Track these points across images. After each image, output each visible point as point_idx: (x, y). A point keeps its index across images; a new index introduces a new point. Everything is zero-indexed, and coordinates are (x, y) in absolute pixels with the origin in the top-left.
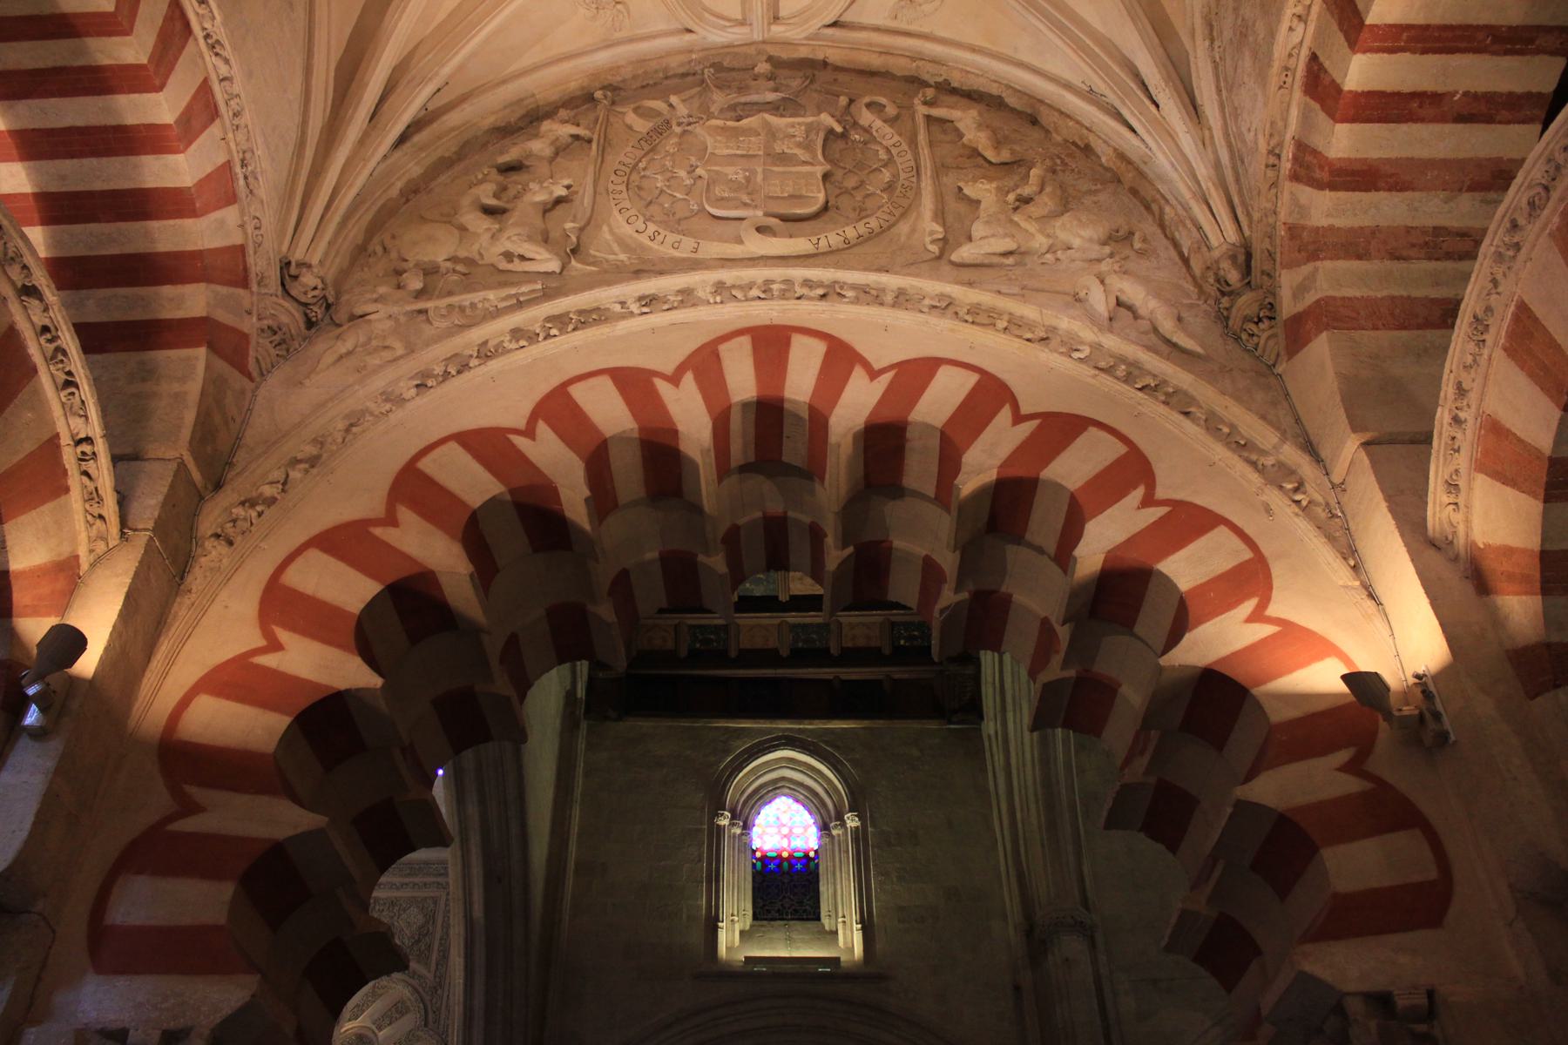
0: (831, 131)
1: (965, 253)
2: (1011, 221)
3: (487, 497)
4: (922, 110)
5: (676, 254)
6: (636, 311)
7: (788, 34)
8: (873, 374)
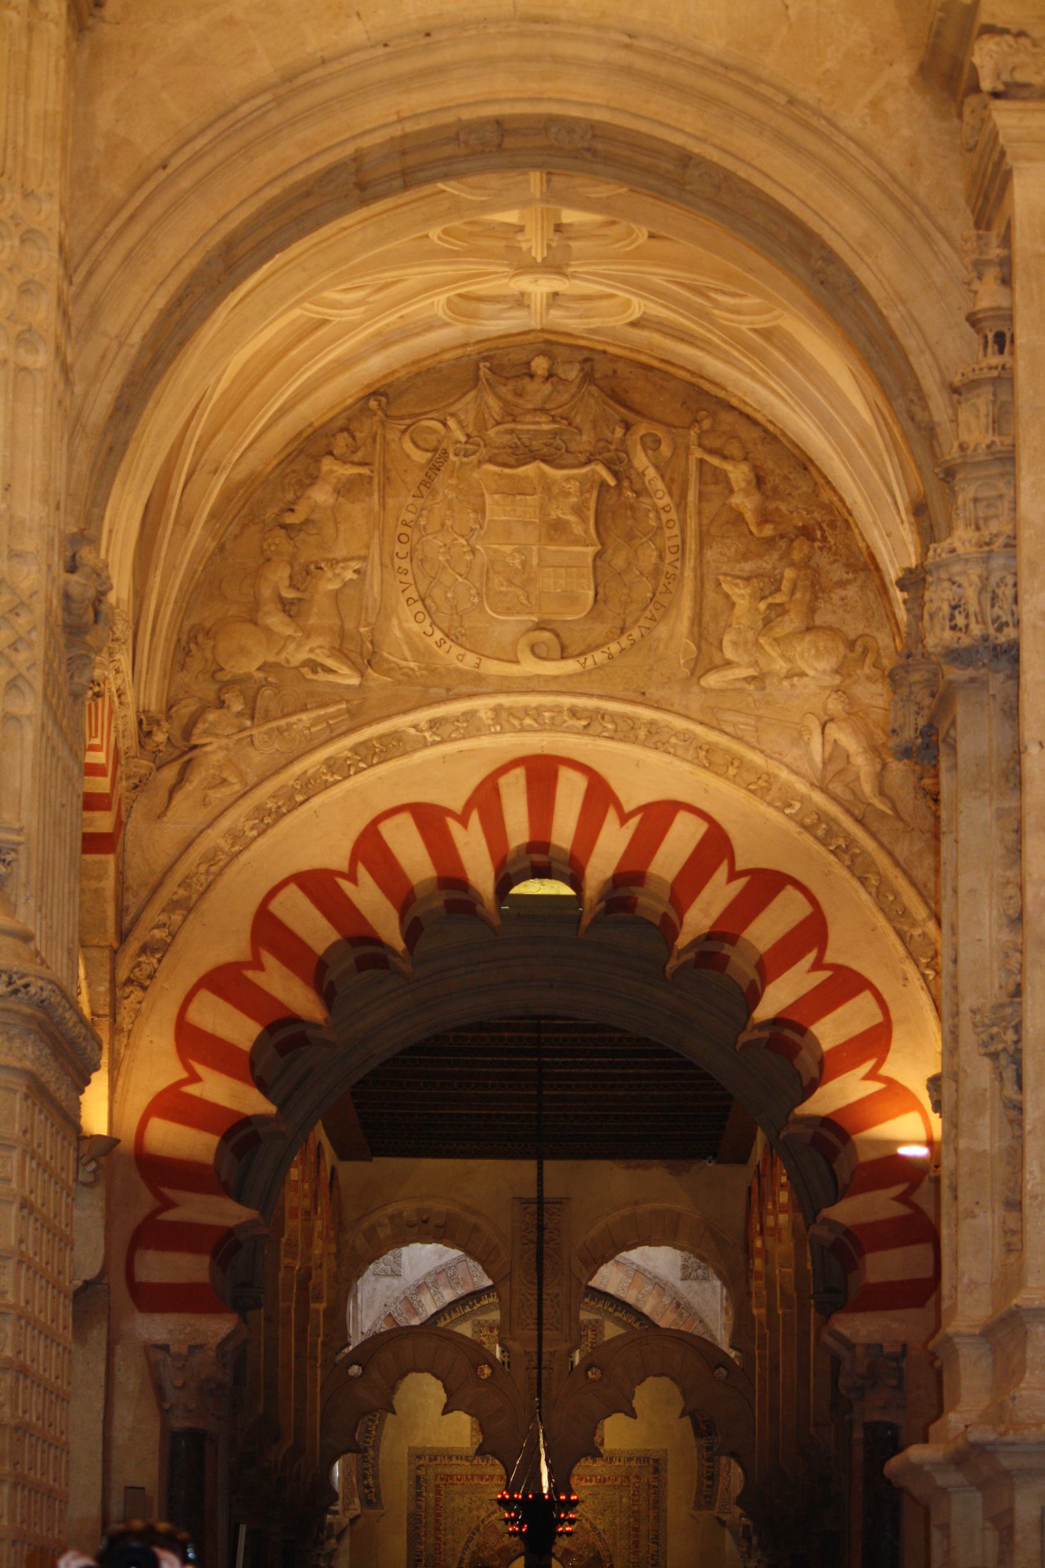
0: (603, 484)
2: (757, 643)
3: (327, 944)
4: (698, 453)
5: (460, 665)
7: (568, 321)
8: (624, 818)
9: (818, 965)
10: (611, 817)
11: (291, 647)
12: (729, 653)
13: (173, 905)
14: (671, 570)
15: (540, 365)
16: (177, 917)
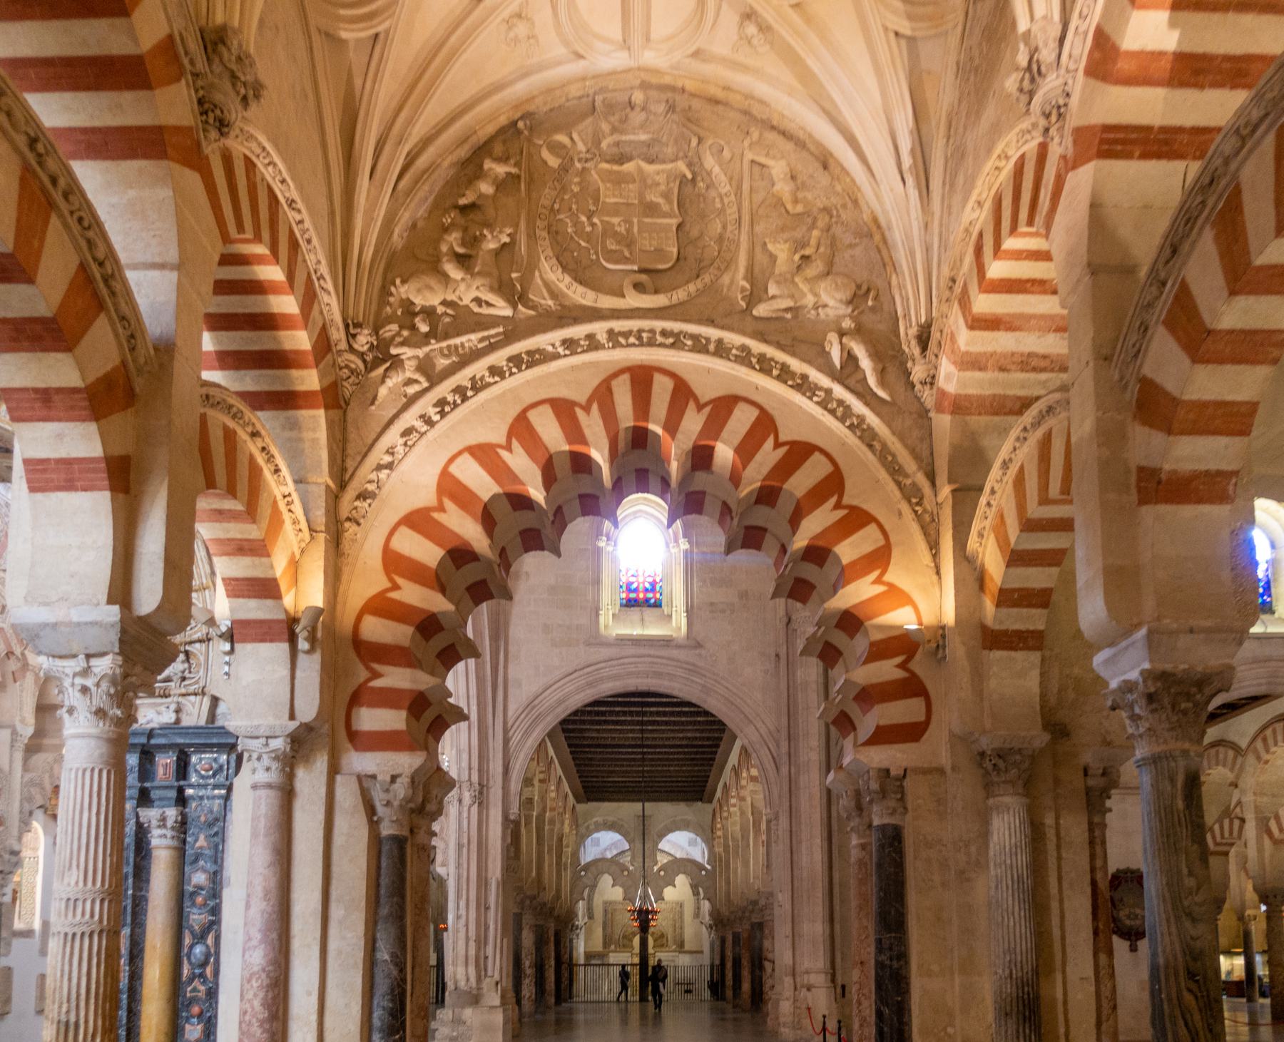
1: (761, 310)
2: (793, 282)
3: (491, 494)
5: (584, 302)
6: (562, 353)
8: (700, 408)
9: (838, 506)
10: (692, 405)
11: (462, 287)
12: (773, 290)
13: (380, 467)
14: (731, 237)
15: (638, 97)
16: (383, 474)
